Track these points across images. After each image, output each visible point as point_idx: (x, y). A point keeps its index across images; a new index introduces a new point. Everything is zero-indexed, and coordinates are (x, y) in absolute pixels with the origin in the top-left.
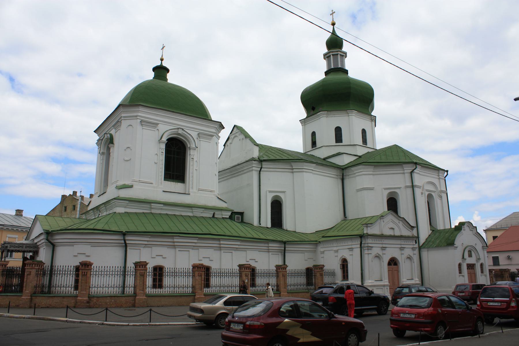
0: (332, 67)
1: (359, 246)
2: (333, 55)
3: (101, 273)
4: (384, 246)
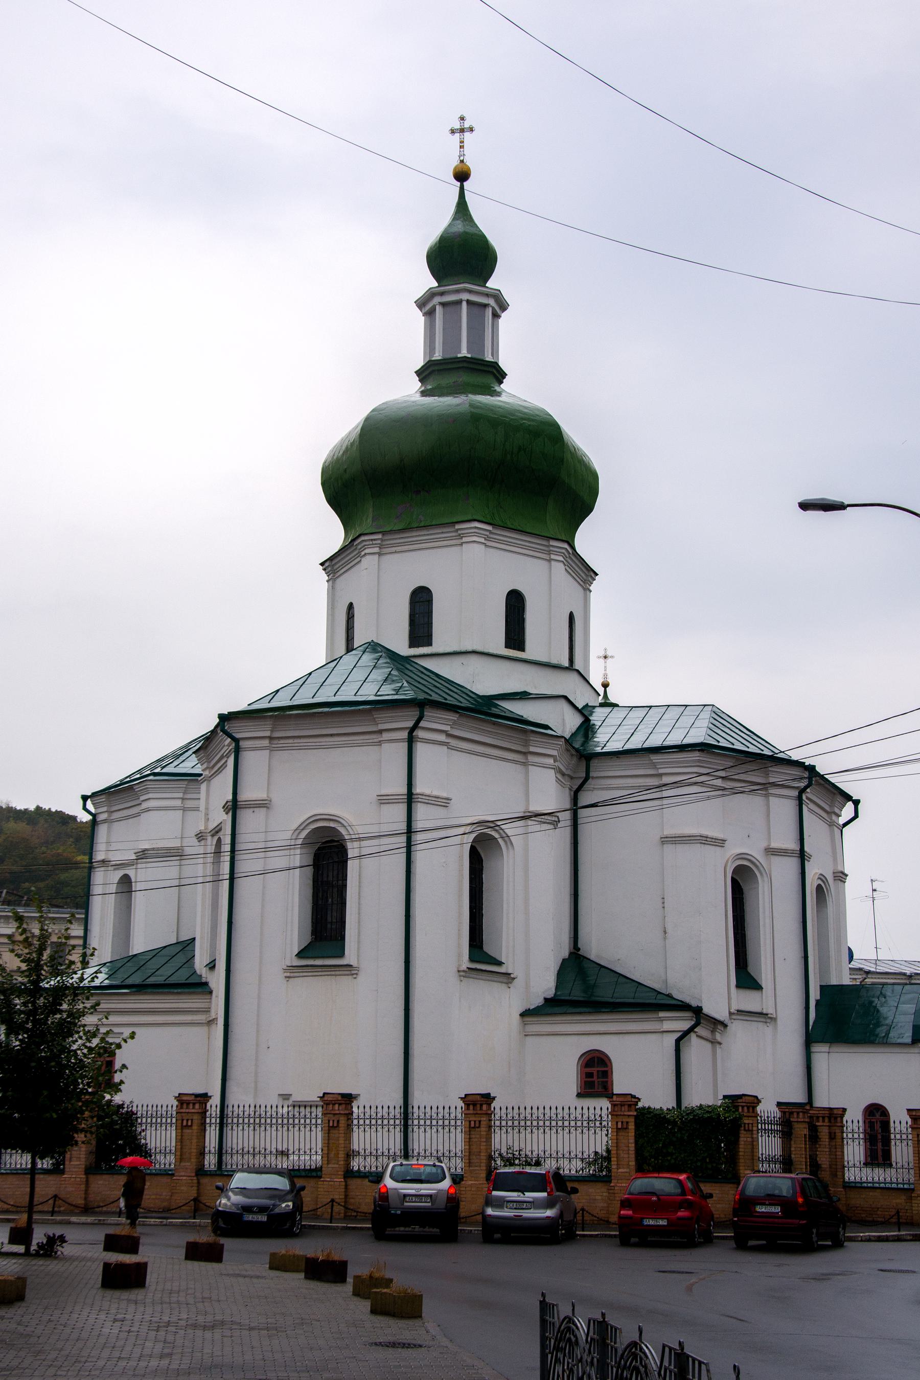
0: (464, 352)
2: (468, 302)
3: (382, 1122)
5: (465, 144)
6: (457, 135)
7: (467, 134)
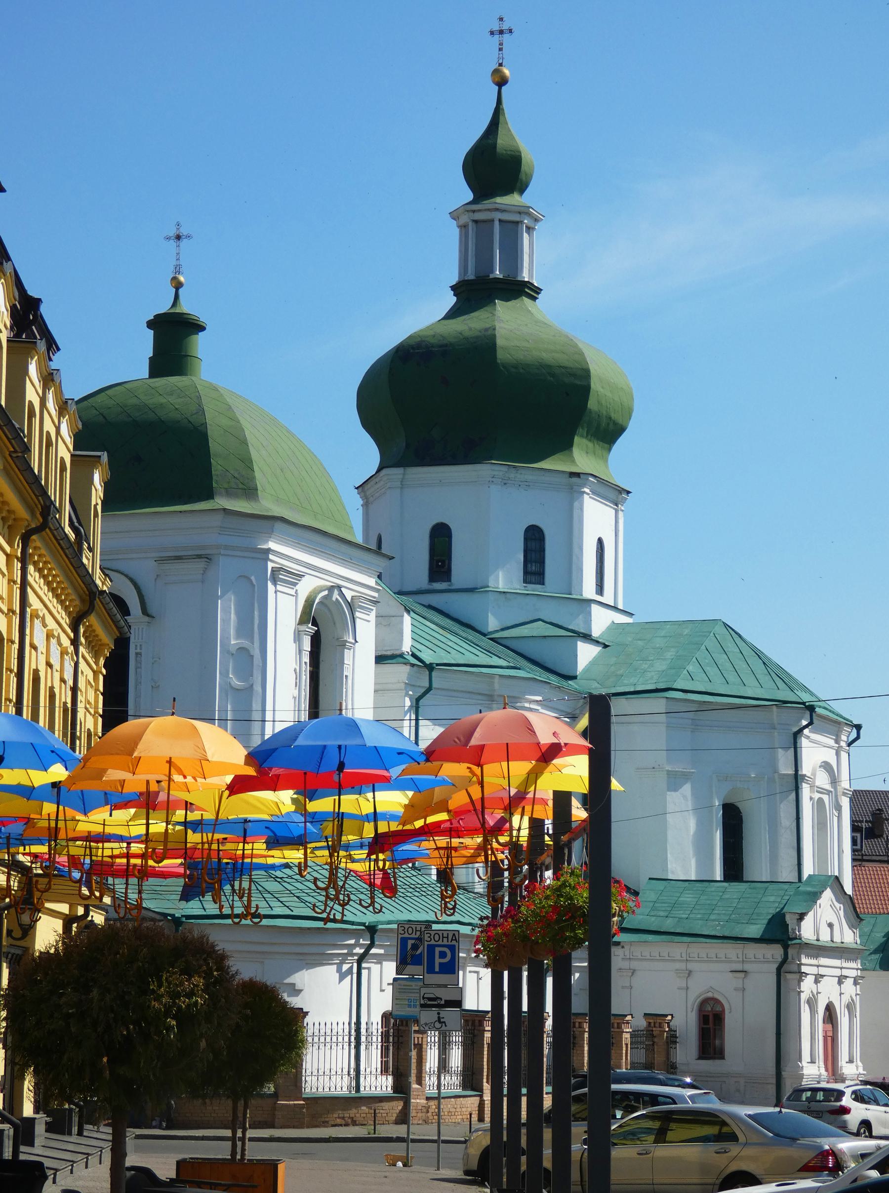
1: (775, 966)
2: (500, 221)
4: (822, 971)
5: (504, 47)
6: (497, 37)
7: (506, 36)
